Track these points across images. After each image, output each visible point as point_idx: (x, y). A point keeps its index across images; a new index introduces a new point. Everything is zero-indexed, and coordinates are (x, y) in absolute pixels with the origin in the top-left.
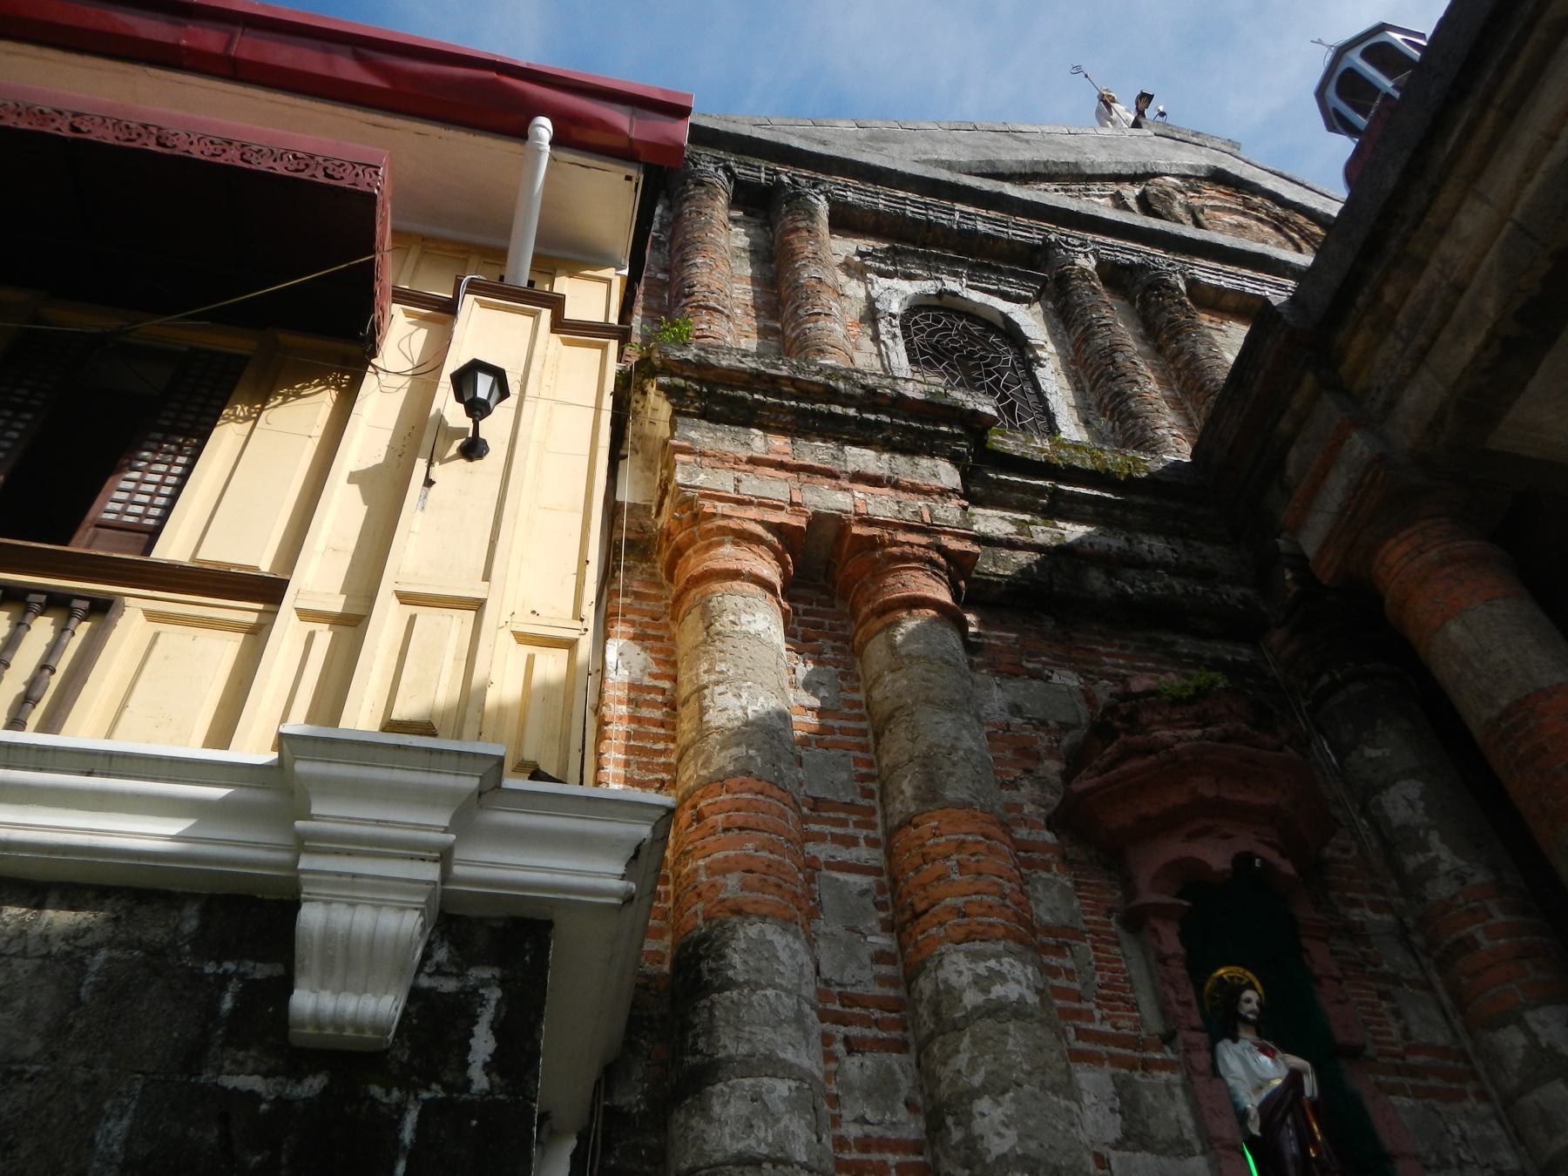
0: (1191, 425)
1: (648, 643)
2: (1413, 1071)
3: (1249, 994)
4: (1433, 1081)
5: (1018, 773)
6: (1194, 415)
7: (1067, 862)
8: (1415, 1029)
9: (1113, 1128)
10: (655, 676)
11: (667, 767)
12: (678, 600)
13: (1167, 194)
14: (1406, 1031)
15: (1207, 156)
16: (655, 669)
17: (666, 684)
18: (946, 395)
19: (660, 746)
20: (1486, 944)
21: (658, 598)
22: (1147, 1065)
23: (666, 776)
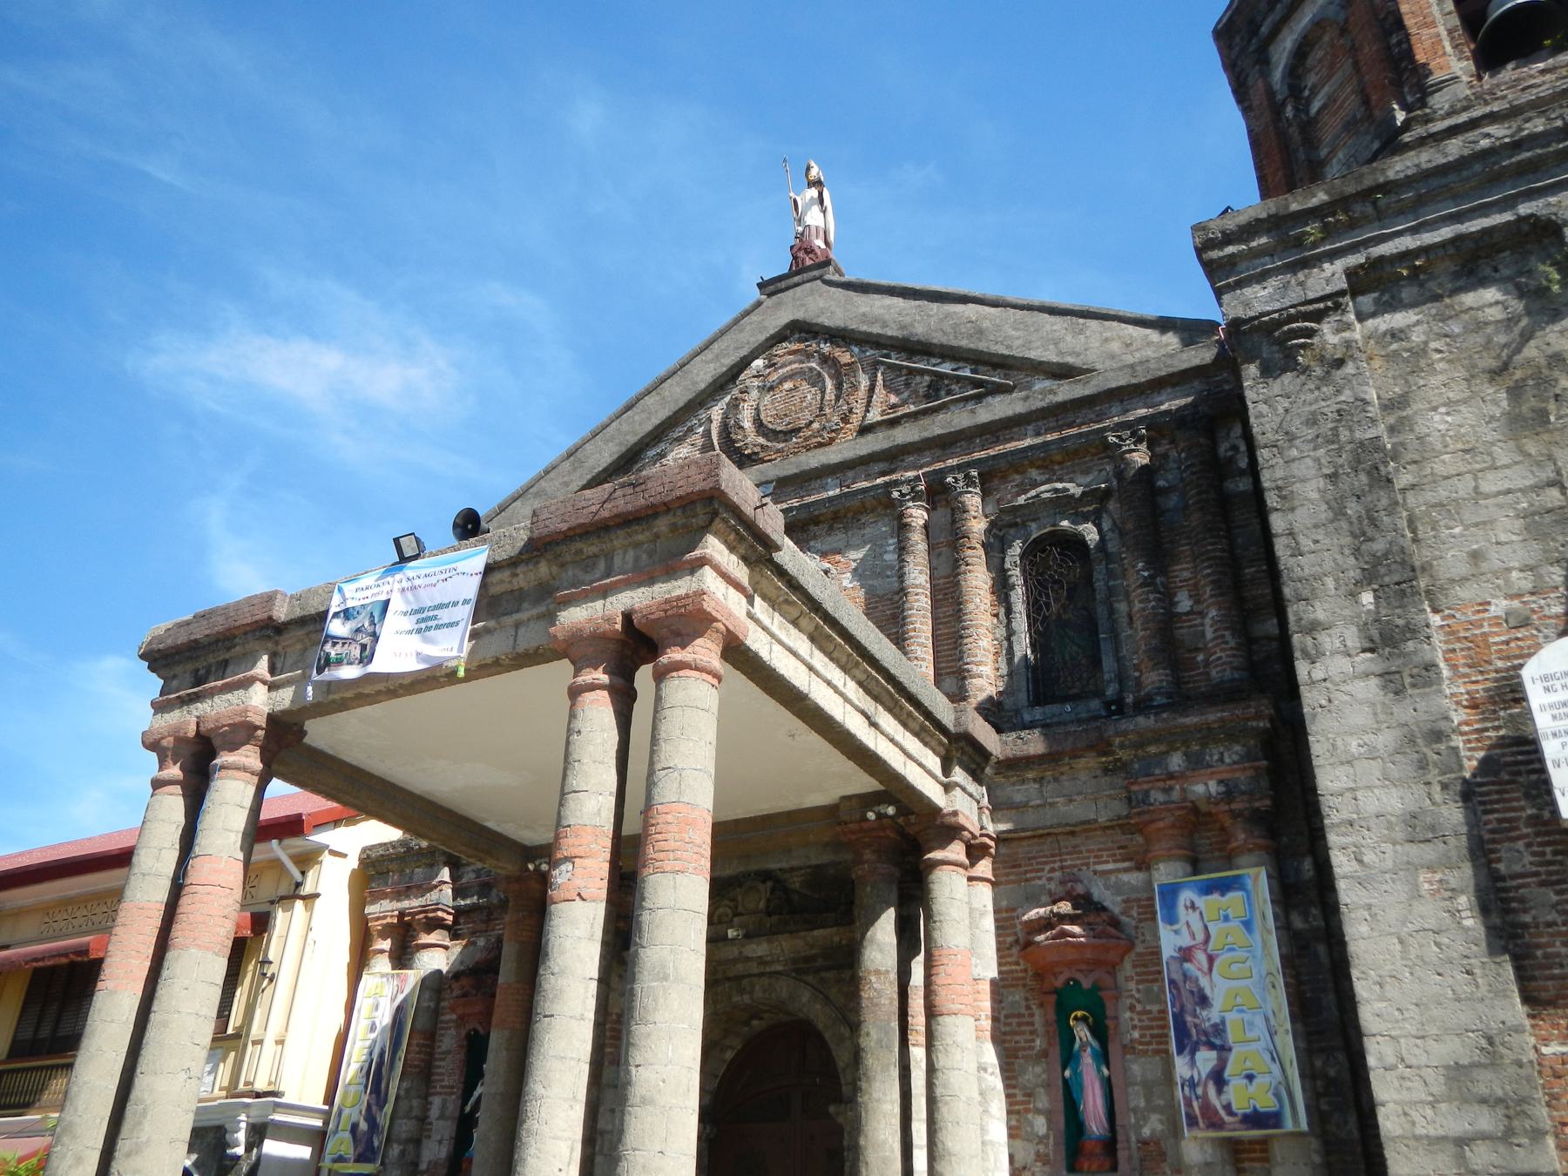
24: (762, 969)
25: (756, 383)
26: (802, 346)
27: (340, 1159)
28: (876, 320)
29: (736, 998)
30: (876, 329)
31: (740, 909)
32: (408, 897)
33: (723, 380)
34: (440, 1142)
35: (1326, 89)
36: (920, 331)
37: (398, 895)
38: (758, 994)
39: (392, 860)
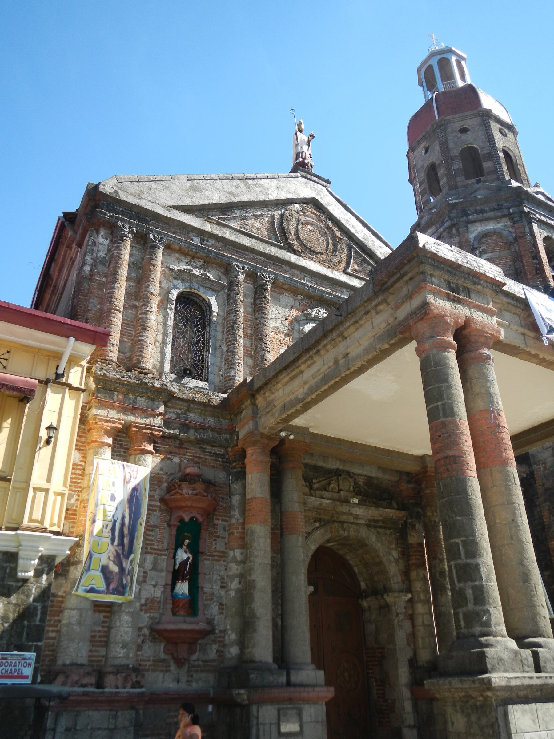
0: (252, 346)
1: (81, 451)
2: (213, 556)
3: (187, 541)
4: (216, 558)
5: (157, 487)
6: (253, 342)
7: (161, 510)
8: (217, 547)
9: (151, 567)
10: (81, 461)
11: (80, 487)
12: (89, 444)
13: (292, 215)
14: (215, 548)
15: (316, 190)
16: (81, 459)
17: (83, 464)
18: (166, 385)
19: (79, 481)
20: (235, 534)
21: (84, 437)
22: (161, 555)
23: (80, 489)
24: (355, 521)
25: (296, 216)
26: (318, 213)
27: (92, 590)
28: (353, 227)
29: (342, 532)
30: (353, 231)
31: (341, 487)
32: (133, 414)
33: (280, 202)
34: (155, 586)
35: (490, 254)
36: (370, 245)
37: (124, 410)
38: (352, 533)
39: (123, 384)
